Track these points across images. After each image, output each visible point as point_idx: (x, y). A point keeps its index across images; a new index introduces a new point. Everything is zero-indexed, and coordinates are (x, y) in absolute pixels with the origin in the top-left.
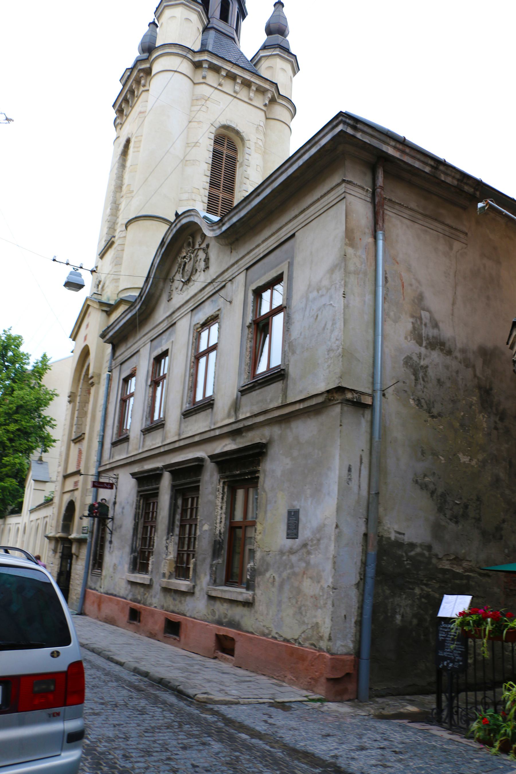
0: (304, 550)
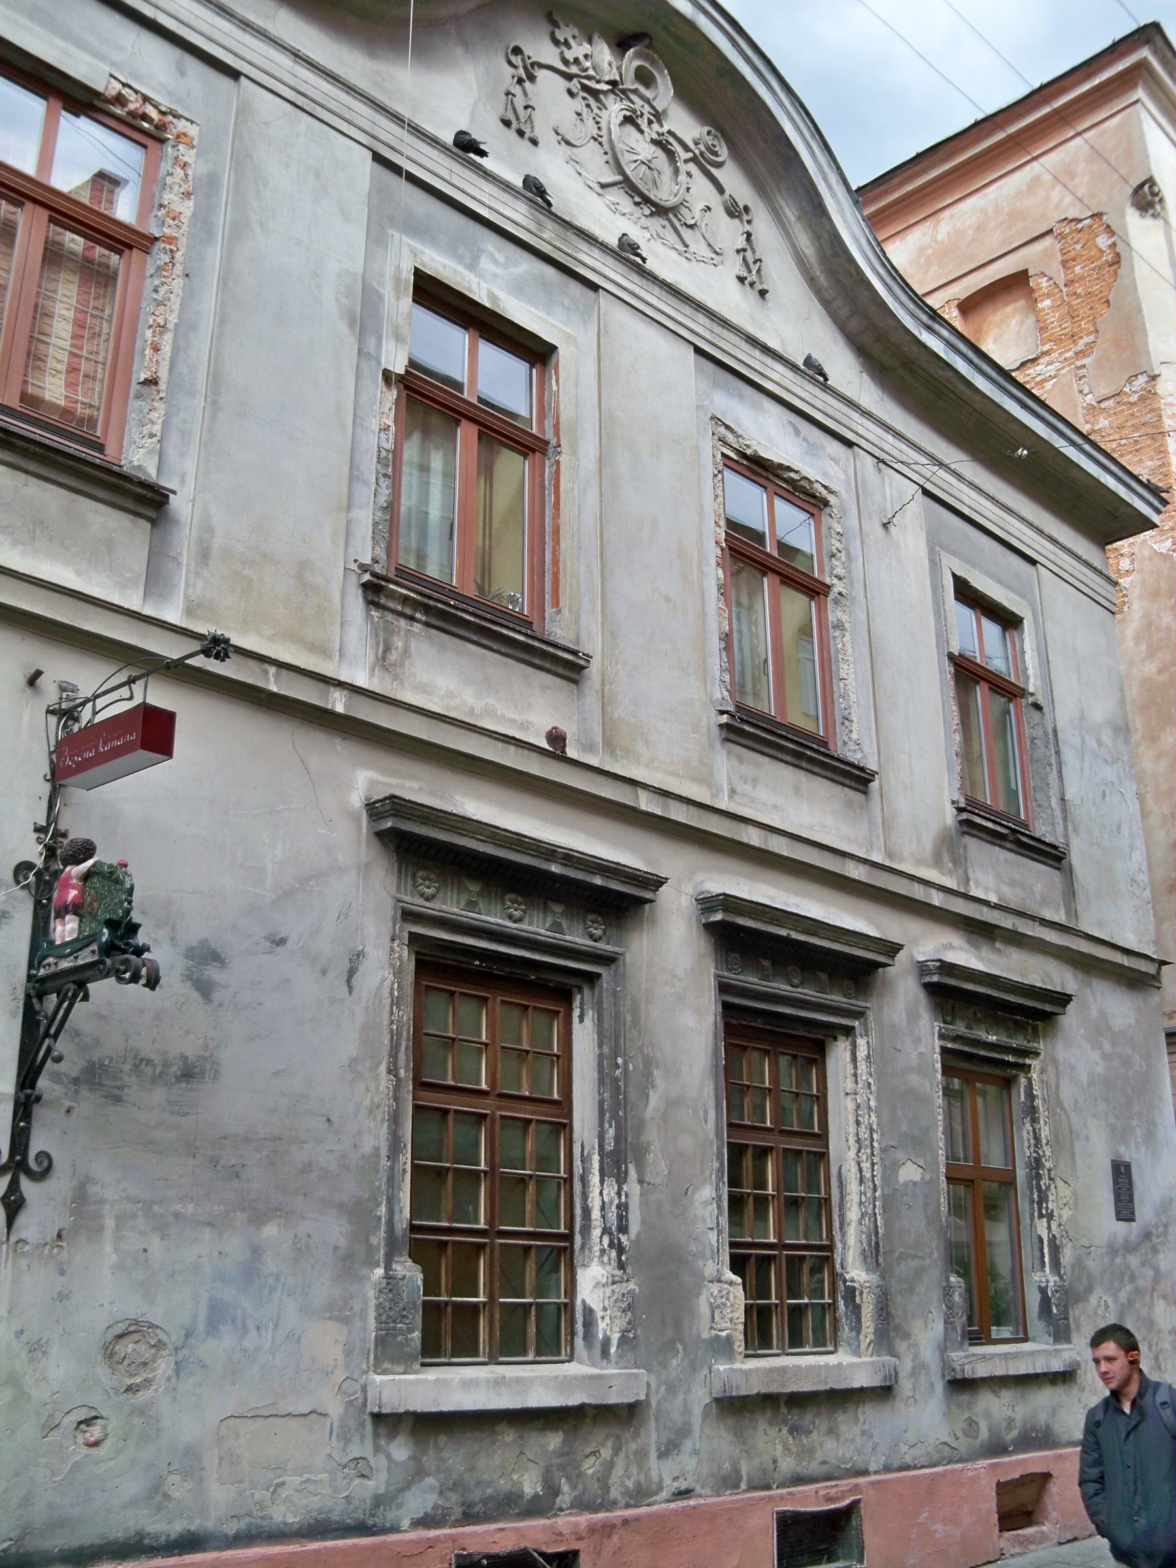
0: (1148, 1245)
